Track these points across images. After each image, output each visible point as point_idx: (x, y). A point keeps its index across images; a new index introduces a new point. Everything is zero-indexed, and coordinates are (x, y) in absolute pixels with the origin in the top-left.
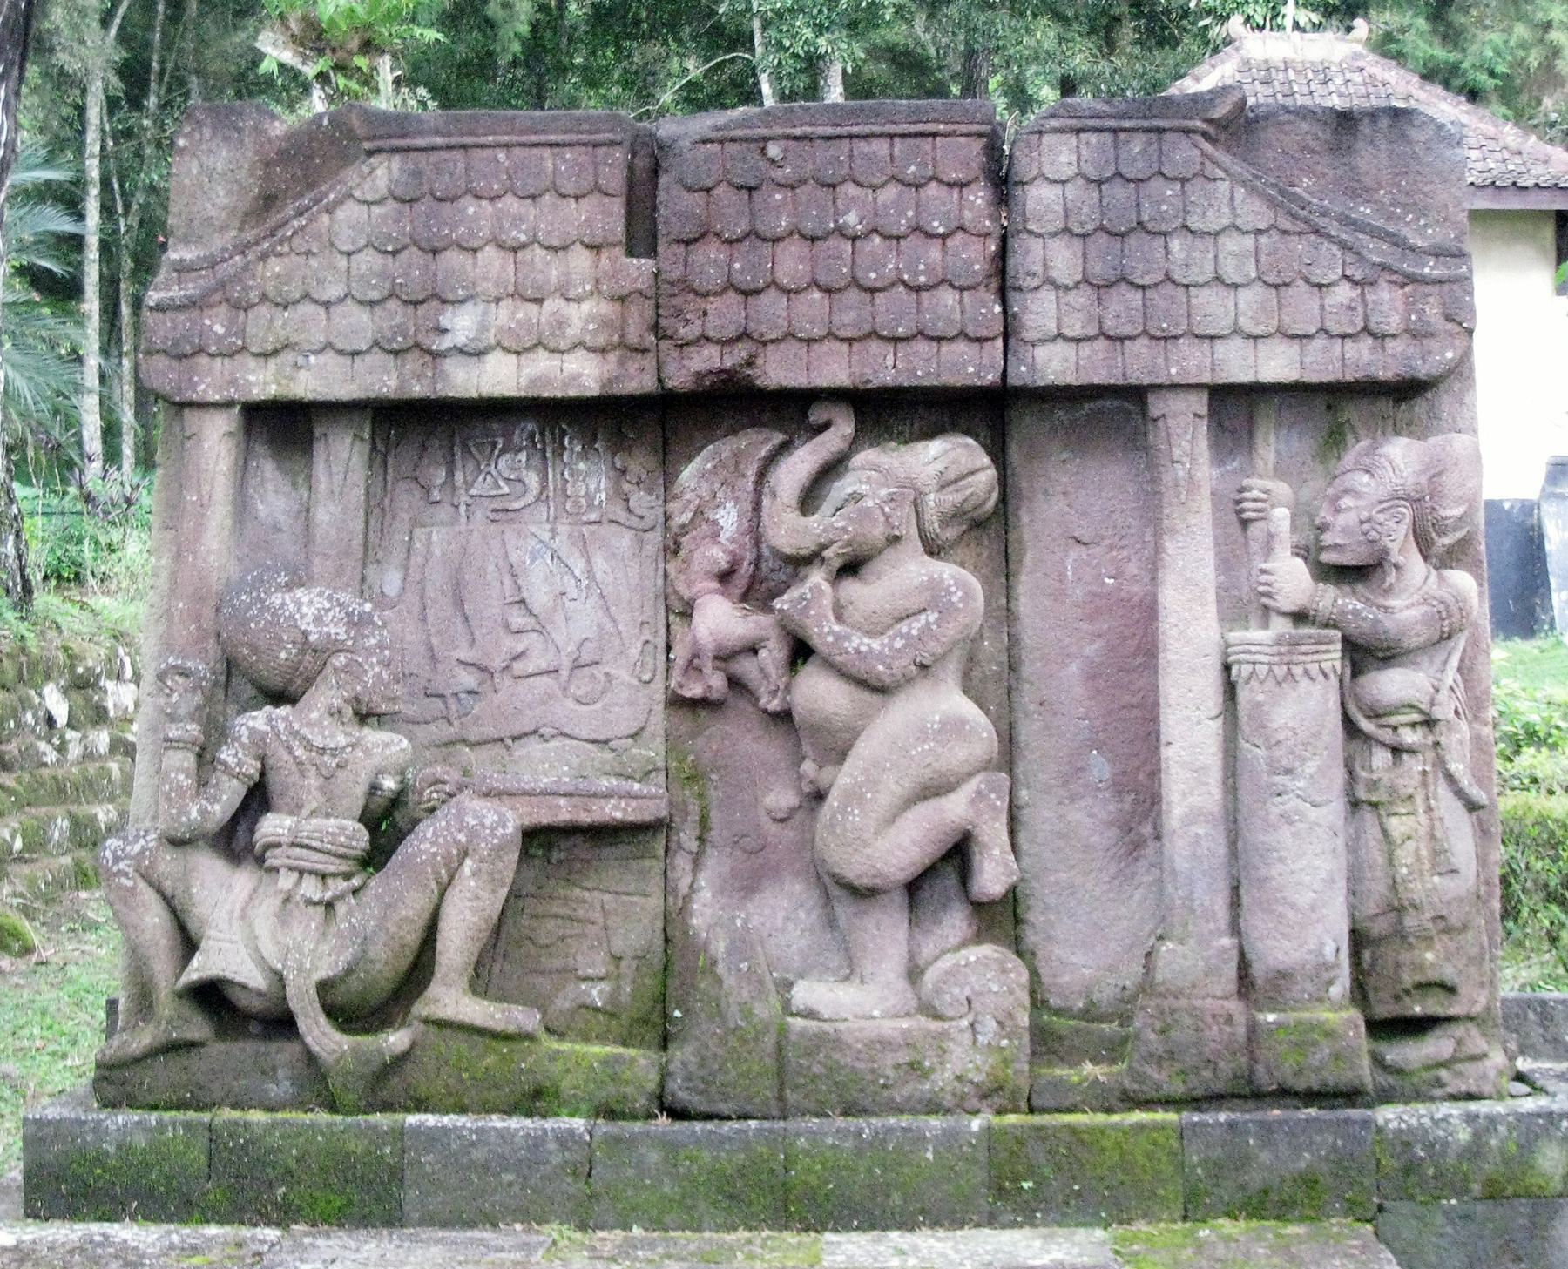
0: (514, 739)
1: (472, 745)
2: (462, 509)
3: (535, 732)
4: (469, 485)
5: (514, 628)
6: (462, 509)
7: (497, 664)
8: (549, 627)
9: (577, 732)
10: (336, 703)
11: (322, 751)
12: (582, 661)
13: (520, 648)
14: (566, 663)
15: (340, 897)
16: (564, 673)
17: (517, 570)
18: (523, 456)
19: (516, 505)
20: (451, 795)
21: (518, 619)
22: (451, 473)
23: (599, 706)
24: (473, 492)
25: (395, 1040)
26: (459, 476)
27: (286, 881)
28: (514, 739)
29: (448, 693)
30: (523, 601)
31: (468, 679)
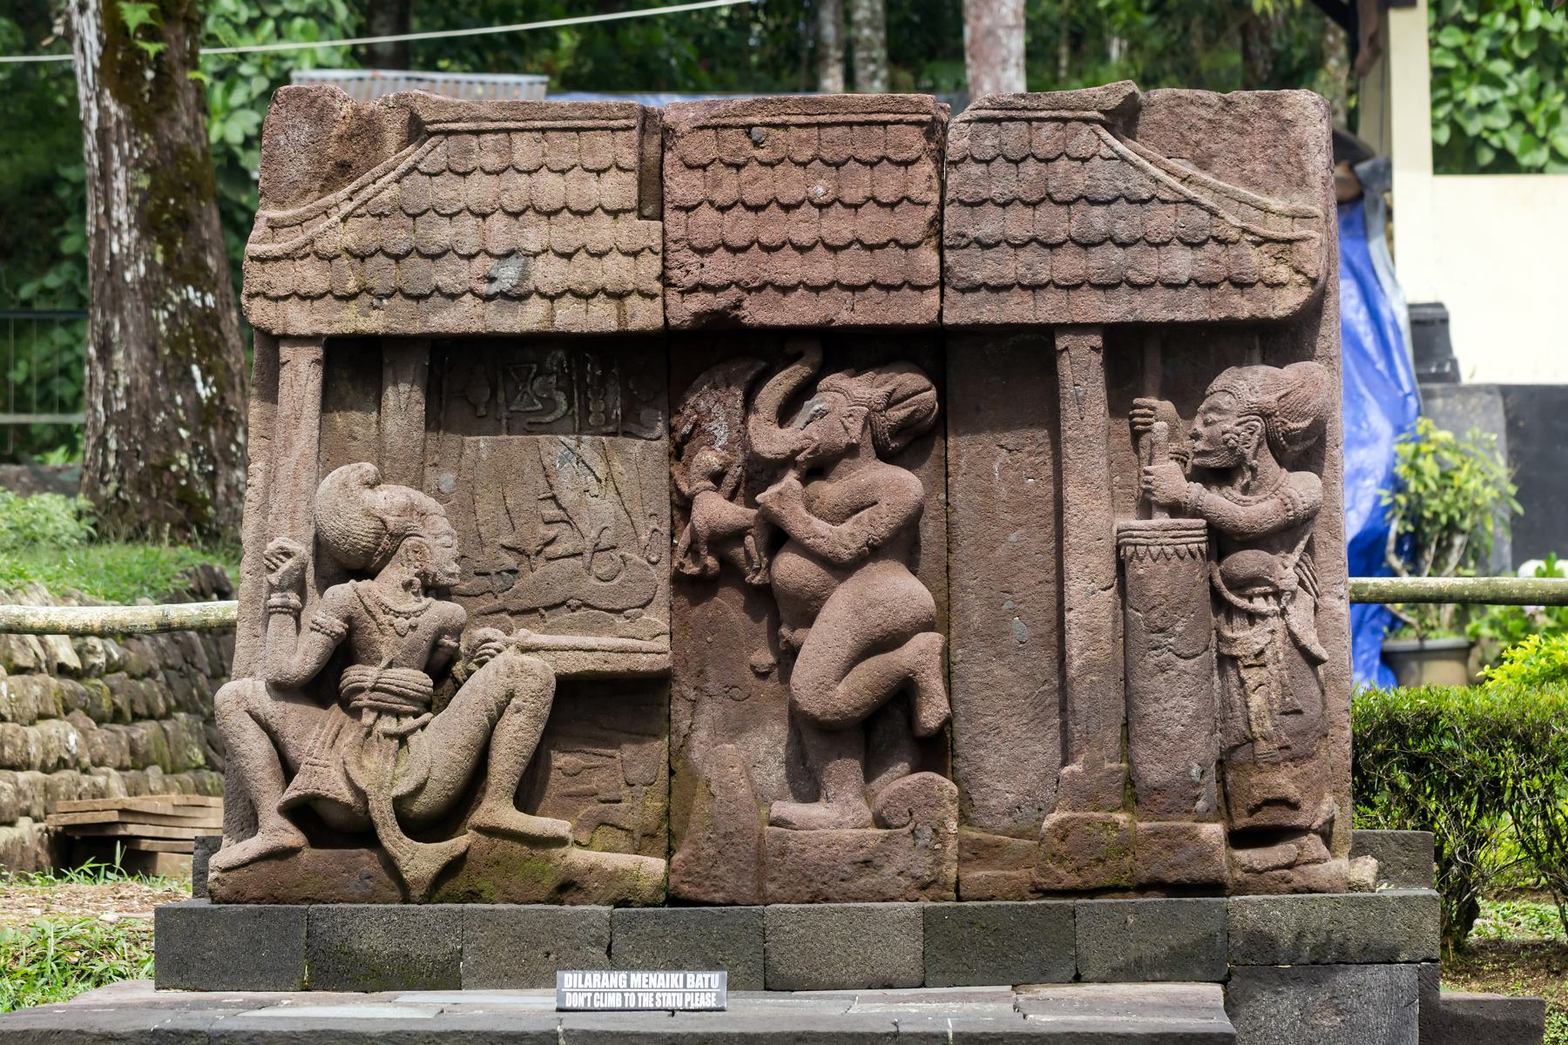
0: (547, 608)
1: (512, 614)
2: (504, 422)
3: (564, 603)
4: (508, 403)
5: (547, 518)
6: (504, 422)
7: (532, 547)
8: (576, 519)
9: (598, 603)
10: (407, 577)
11: (398, 614)
12: (601, 546)
13: (552, 534)
14: (589, 545)
15: (413, 731)
16: (588, 555)
17: (550, 471)
18: (553, 379)
19: (548, 419)
20: (499, 651)
21: (551, 511)
22: (494, 395)
23: (616, 582)
24: (513, 408)
25: (458, 843)
26: (501, 396)
27: (368, 718)
28: (547, 608)
29: (492, 571)
30: (554, 498)
31: (510, 561)
